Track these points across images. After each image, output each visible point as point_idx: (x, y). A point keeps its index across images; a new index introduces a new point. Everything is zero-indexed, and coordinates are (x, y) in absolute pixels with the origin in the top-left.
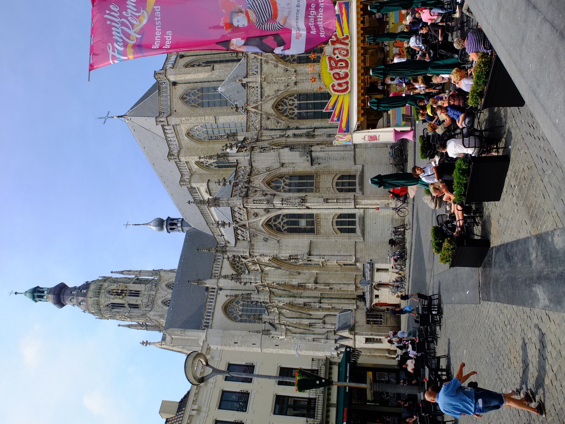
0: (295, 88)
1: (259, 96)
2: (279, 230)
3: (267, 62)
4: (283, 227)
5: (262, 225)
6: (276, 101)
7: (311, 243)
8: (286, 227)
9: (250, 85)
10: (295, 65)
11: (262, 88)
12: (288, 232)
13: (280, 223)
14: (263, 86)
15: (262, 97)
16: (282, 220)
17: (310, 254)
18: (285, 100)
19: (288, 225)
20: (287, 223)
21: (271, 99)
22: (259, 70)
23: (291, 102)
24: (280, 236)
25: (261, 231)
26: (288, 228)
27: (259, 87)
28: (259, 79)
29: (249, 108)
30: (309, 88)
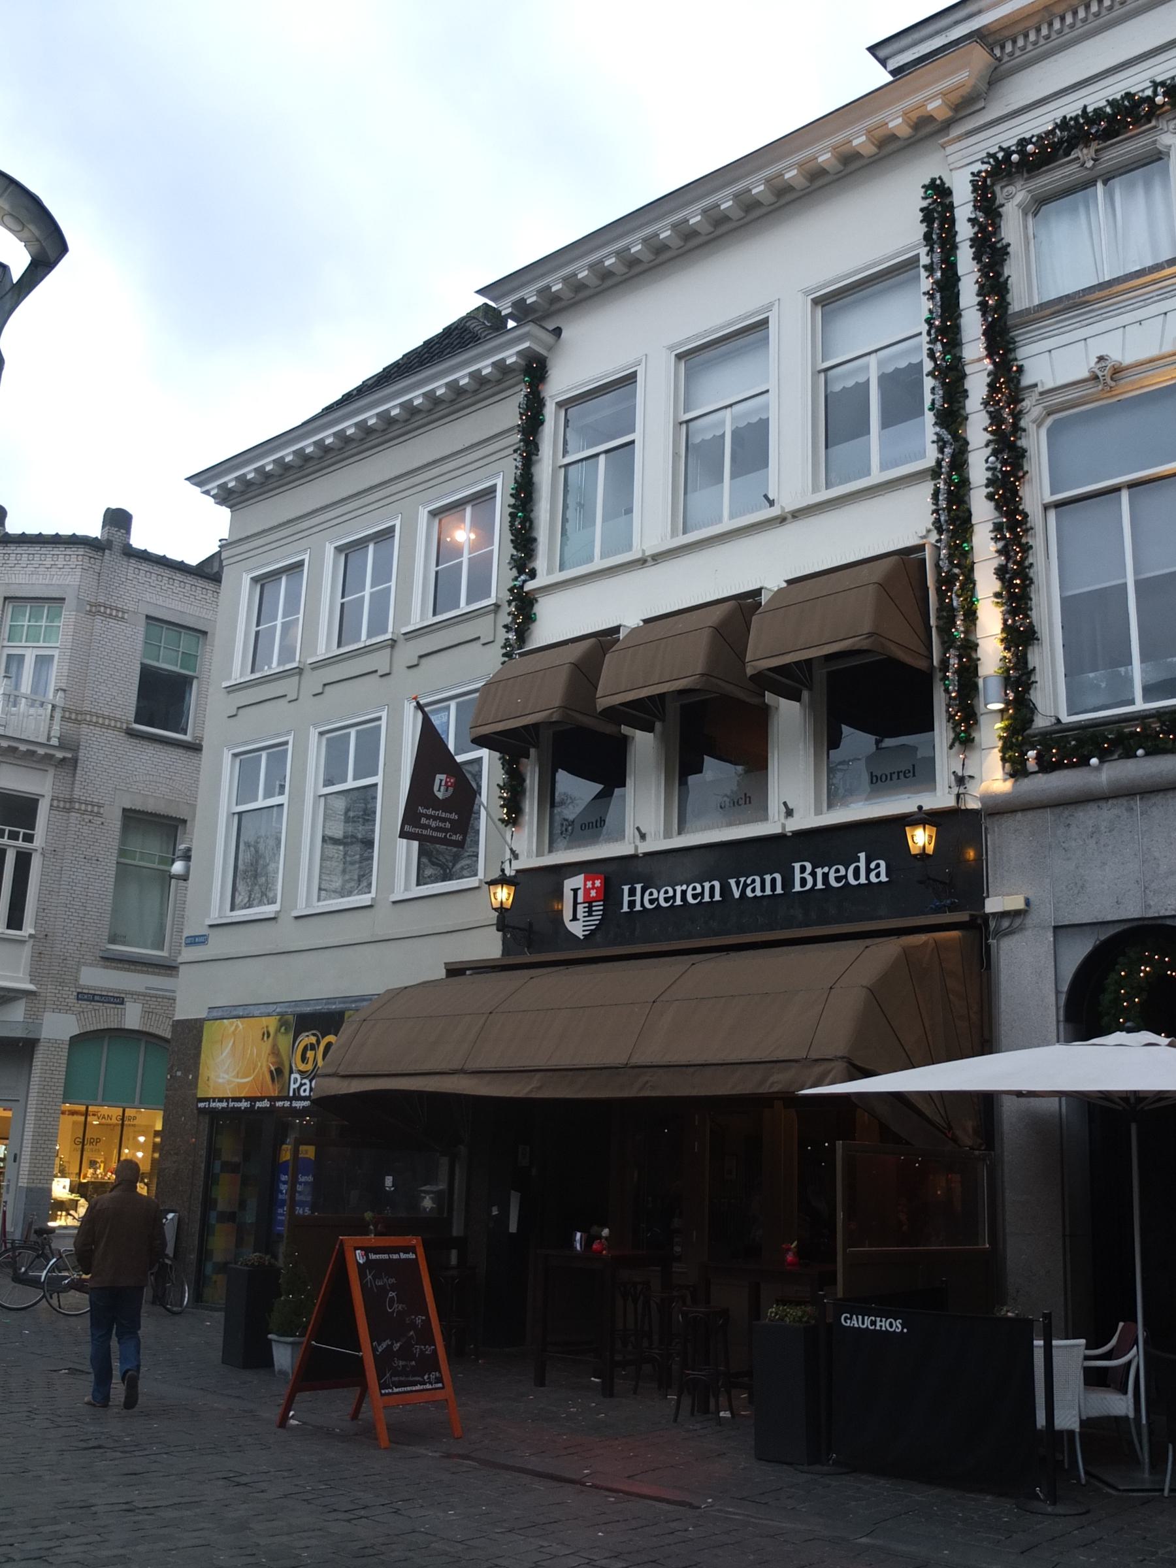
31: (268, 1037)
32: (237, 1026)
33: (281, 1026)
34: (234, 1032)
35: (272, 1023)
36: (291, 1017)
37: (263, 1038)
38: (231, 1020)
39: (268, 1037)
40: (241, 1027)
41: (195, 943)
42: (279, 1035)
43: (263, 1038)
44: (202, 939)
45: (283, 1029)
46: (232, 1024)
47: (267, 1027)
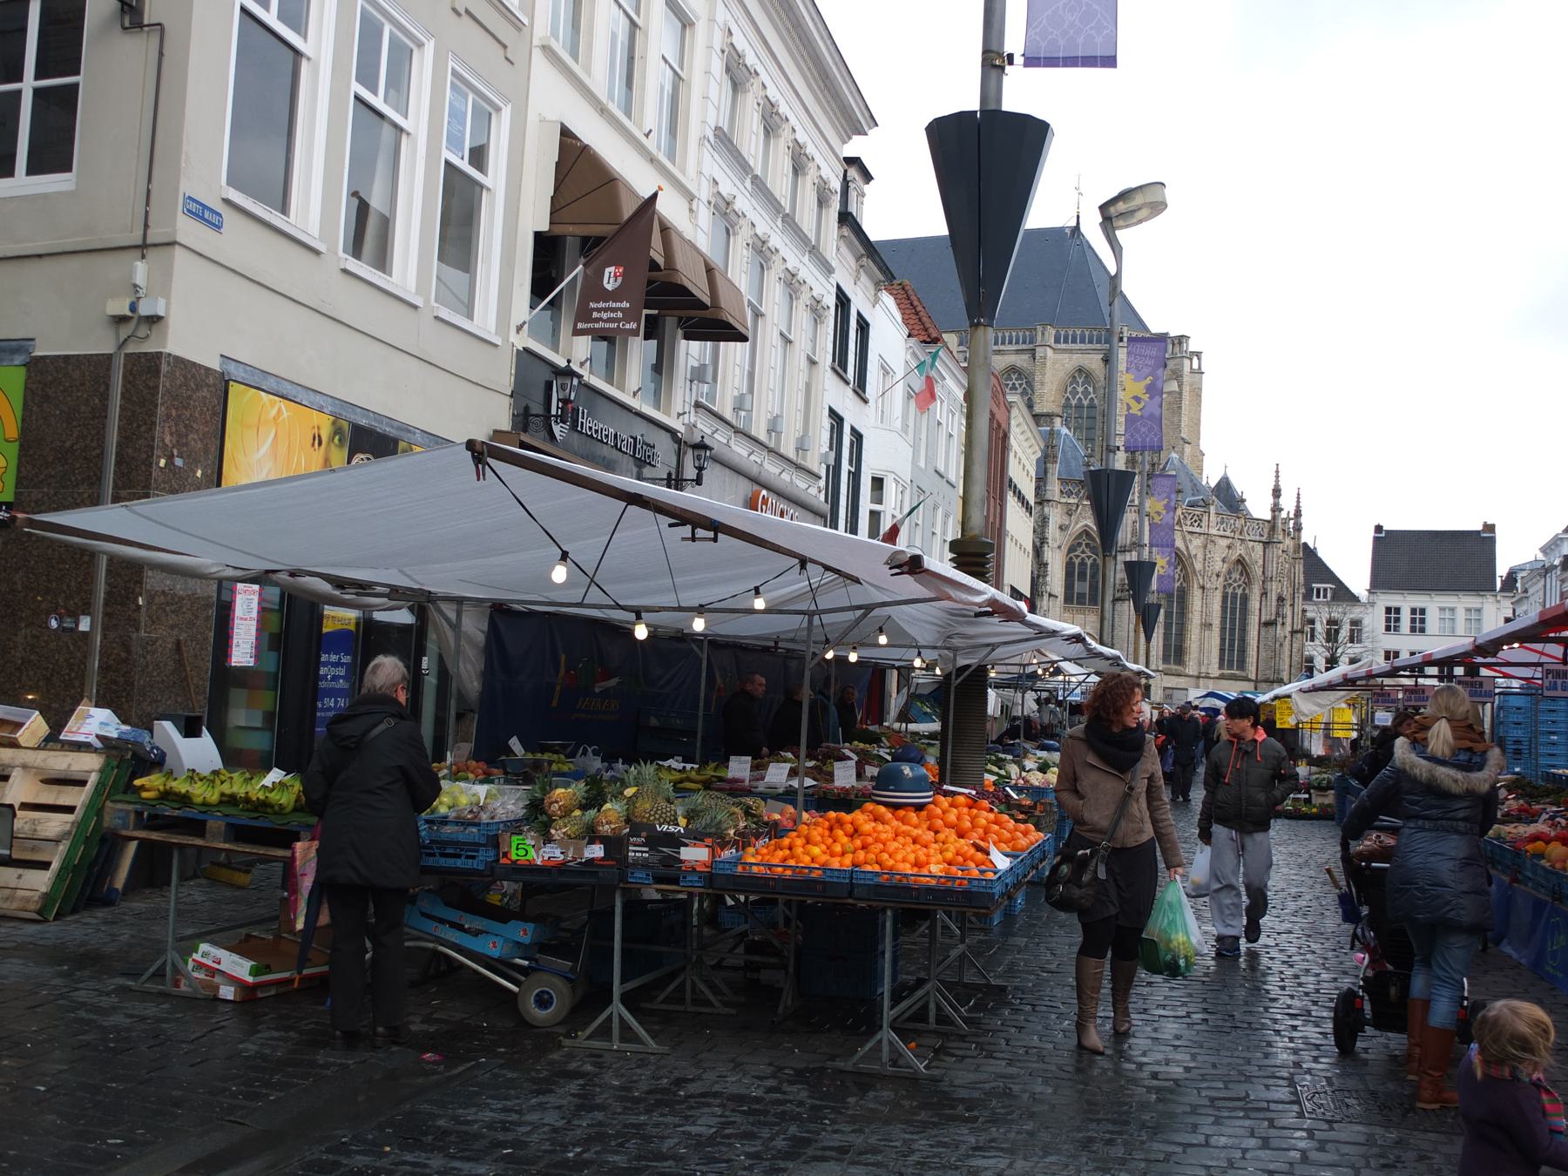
0: (1196, 586)
1: (1191, 529)
2: (1071, 549)
3: (1229, 547)
4: (1077, 556)
5: (1086, 525)
6: (1183, 554)
7: (1057, 597)
8: (1077, 561)
9: (1205, 518)
10: (1221, 588)
11: (1200, 534)
12: (1067, 563)
13: (1083, 552)
14: (1202, 537)
15: (1189, 532)
16: (1089, 557)
17: (1050, 595)
18: (1179, 568)
19: (1092, 565)
20: (1083, 563)
21: (1187, 548)
22: (1222, 533)
23: (1177, 576)
24: (1065, 550)
25: (1077, 523)
26: (1074, 563)
27: (1198, 530)
28: (1213, 531)
29: (1179, 512)
30: (1195, 608)
31: (320, 443)
32: (279, 410)
33: (335, 434)
34: (275, 419)
35: (325, 425)
36: (345, 425)
37: (313, 445)
38: (271, 397)
39: (320, 443)
40: (285, 414)
41: (203, 218)
42: (332, 446)
43: (313, 445)
44: (215, 219)
45: (337, 437)
46: (273, 404)
47: (319, 428)
